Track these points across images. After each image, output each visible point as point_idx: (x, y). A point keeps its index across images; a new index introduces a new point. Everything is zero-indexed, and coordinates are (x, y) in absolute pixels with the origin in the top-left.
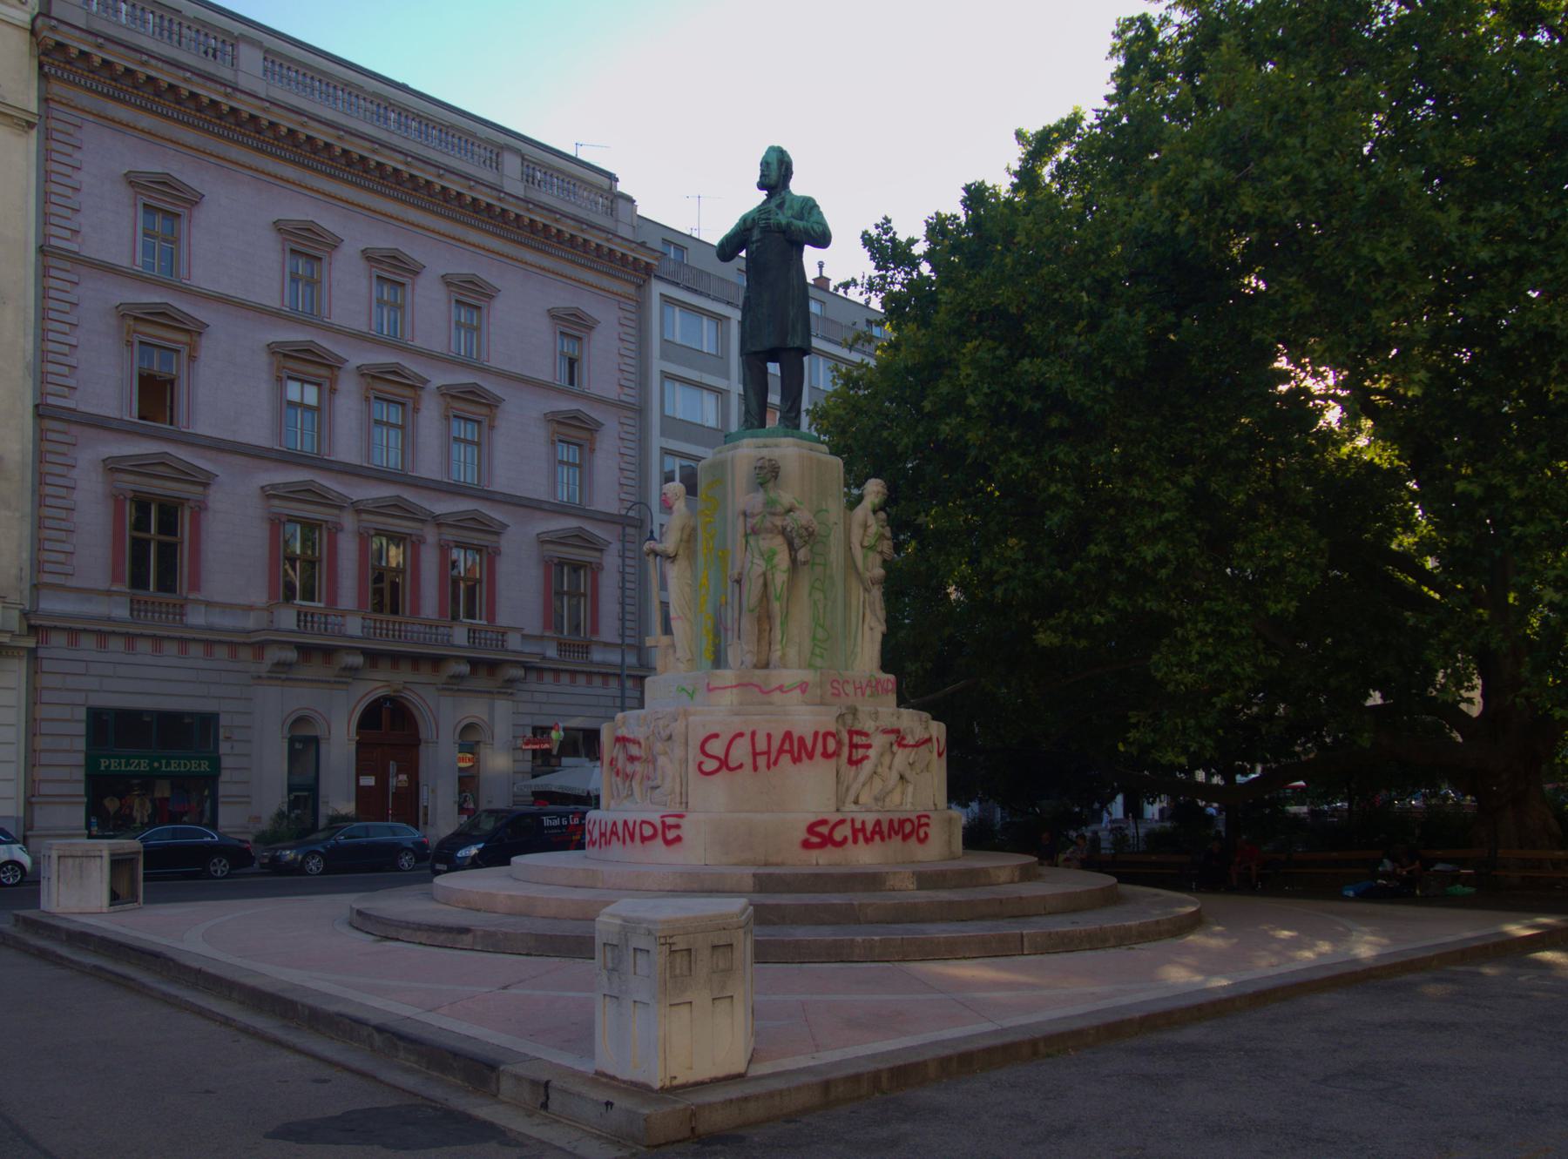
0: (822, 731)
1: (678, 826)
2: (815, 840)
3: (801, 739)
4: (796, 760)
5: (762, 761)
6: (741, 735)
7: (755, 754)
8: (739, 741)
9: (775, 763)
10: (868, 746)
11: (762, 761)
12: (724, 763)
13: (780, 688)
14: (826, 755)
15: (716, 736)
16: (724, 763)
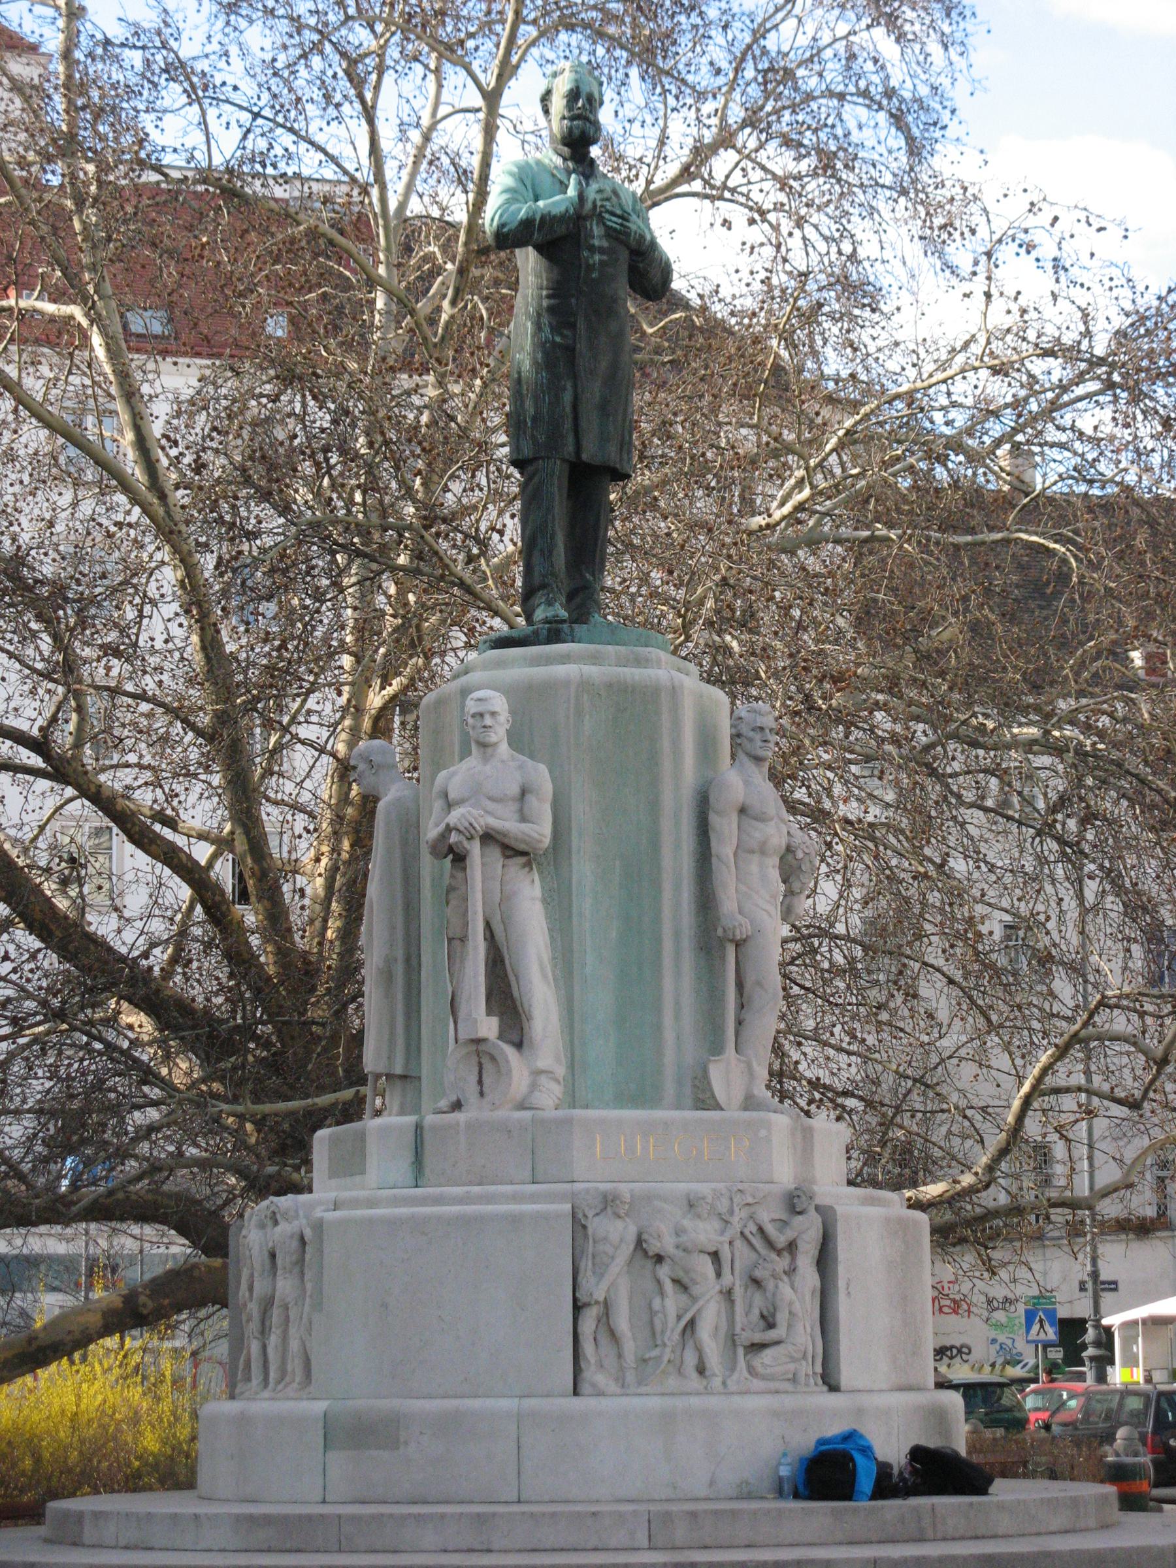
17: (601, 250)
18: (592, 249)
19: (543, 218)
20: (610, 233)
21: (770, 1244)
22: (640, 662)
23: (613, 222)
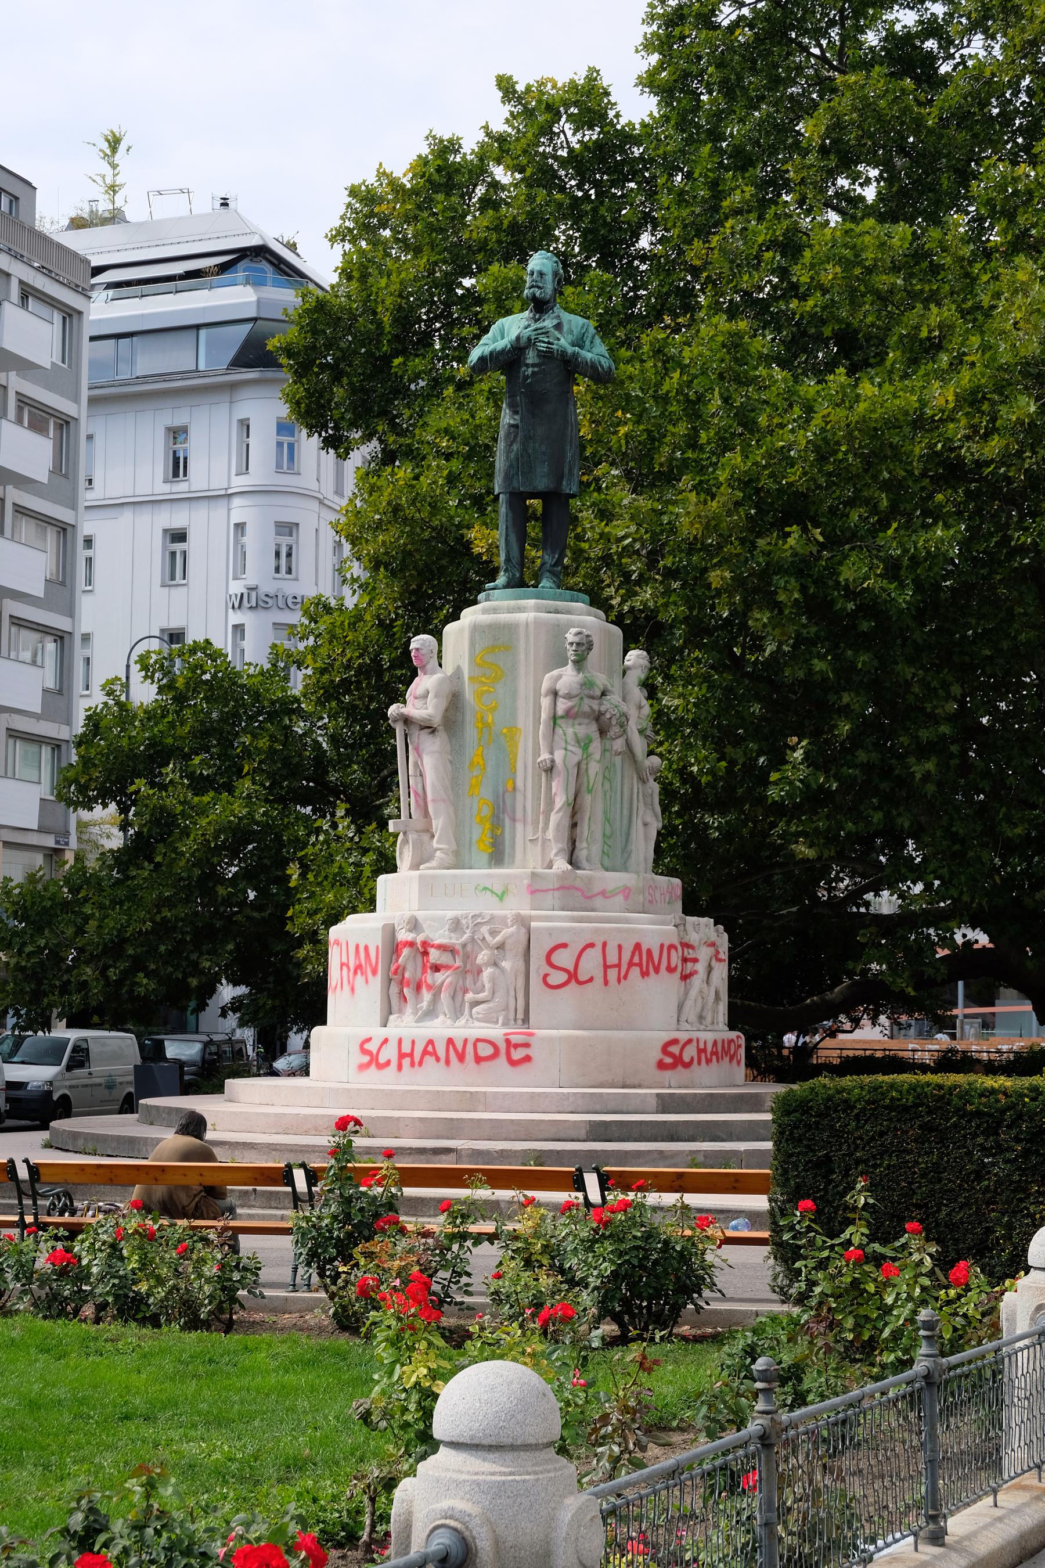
0: (667, 944)
1: (527, 1045)
2: (668, 1060)
3: (649, 952)
4: (645, 974)
5: (613, 974)
6: (591, 945)
7: (606, 967)
8: (589, 951)
9: (625, 977)
10: (695, 960)
11: (613, 974)
12: (573, 976)
13: (603, 893)
14: (671, 970)
15: (564, 946)
16: (573, 976)
17: (533, 365)
18: (527, 366)
19: (491, 353)
20: (540, 354)
21: (488, 946)
22: (520, 609)
23: (542, 347)
